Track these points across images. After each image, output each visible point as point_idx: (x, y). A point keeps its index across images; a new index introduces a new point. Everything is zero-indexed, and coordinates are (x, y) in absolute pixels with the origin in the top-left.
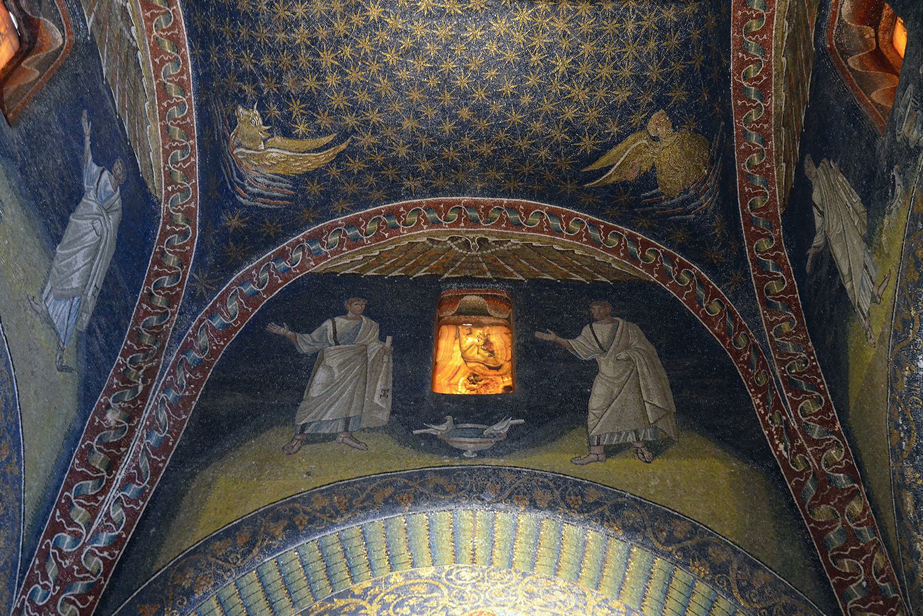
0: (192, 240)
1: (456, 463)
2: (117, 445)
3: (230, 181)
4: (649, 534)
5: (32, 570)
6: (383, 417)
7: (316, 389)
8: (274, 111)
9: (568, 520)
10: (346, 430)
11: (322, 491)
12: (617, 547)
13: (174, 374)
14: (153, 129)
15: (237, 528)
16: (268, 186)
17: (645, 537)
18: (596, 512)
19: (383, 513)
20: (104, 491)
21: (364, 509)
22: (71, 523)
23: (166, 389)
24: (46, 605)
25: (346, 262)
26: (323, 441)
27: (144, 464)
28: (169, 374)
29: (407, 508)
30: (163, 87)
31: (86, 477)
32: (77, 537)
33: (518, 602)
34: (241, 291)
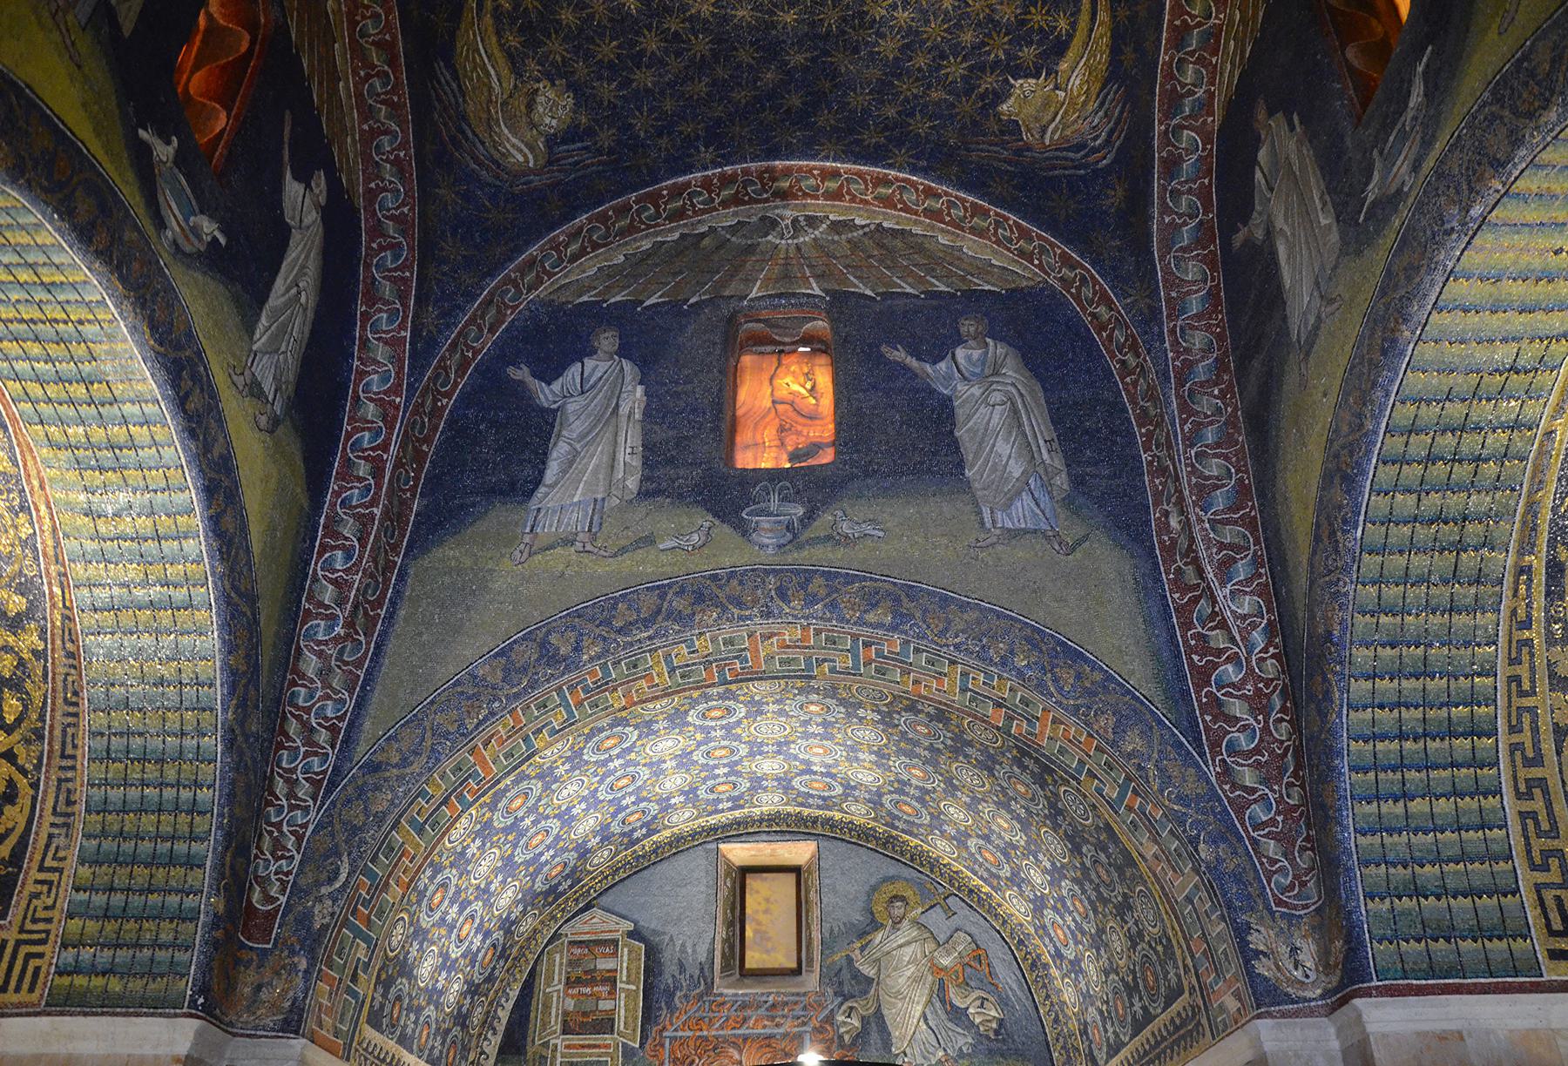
0: (1092, 277)
2: (1190, 546)
3: (1075, 168)
5: (1207, 729)
8: (1028, 53)
14: (970, 246)
15: (1318, 525)
16: (1106, 115)
20: (1214, 602)
22: (1220, 652)
24: (1261, 740)
25: (1229, 74)
26: (1316, 335)
29: (1407, 333)
30: (929, 213)
31: (1196, 600)
32: (1234, 659)
34: (1183, 249)
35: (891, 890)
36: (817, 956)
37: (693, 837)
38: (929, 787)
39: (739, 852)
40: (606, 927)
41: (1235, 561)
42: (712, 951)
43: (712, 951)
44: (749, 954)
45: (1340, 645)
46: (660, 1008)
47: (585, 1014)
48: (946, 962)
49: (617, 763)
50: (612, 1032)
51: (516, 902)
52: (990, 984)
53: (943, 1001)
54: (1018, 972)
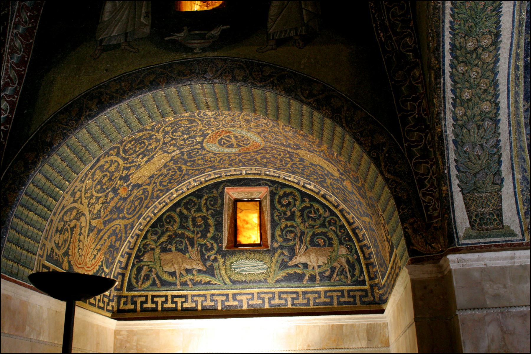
1: (190, 57)
4: (299, 93)
6: (147, 30)
7: (106, 17)
9: (254, 86)
10: (126, 41)
11: (115, 80)
12: (283, 100)
13: (20, 16)
15: (71, 106)
17: (296, 95)
18: (269, 81)
19: (150, 90)
21: (139, 89)
23: (16, 26)
27: (13, 74)
28: (16, 17)
29: (164, 86)
33: (241, 125)
41: (10, 86)
45: (53, 150)
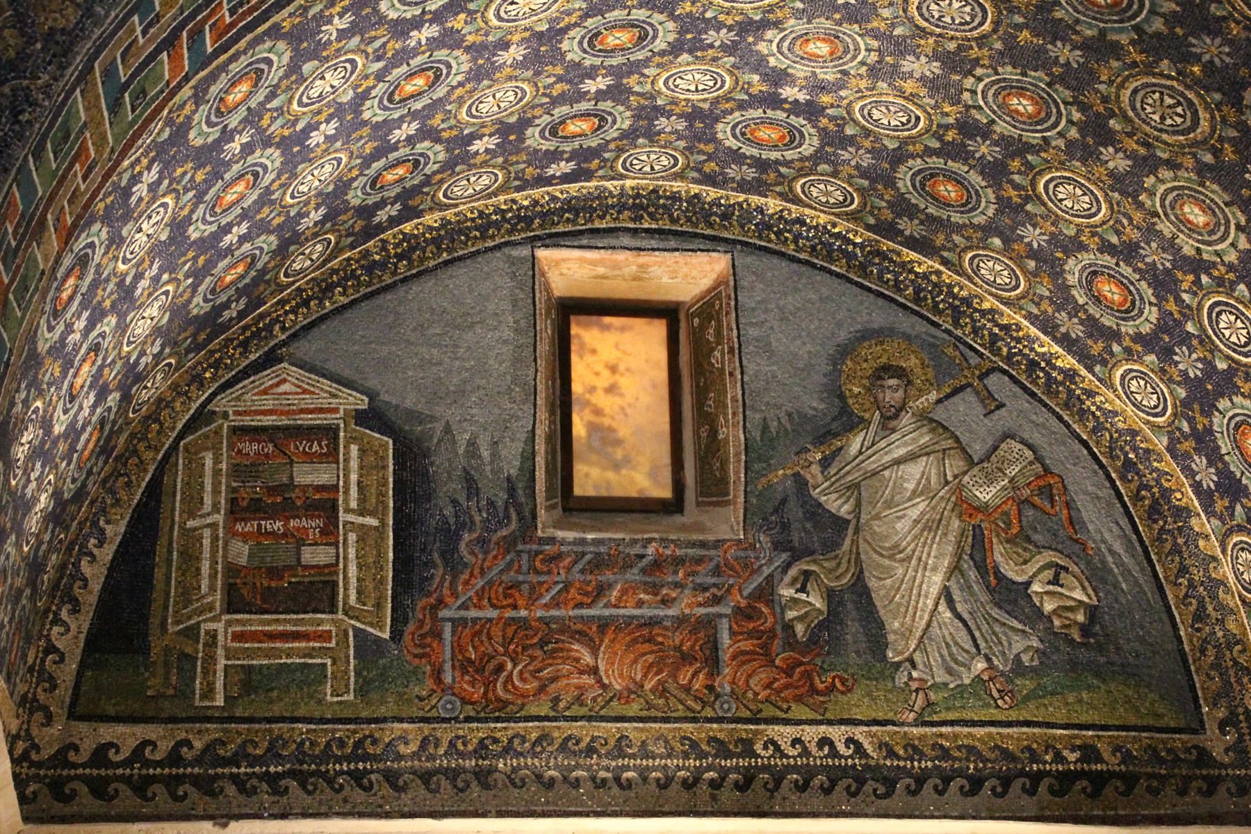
35: (875, 355)
36: (736, 472)
37: (483, 230)
38: (1034, 138)
39: (569, 269)
40: (308, 402)
42: (529, 457)
43: (529, 457)
44: (579, 469)
46: (430, 564)
47: (274, 573)
48: (985, 494)
49: (429, 32)
50: (333, 609)
51: (157, 331)
52: (1072, 542)
53: (981, 568)
54: (1124, 522)
